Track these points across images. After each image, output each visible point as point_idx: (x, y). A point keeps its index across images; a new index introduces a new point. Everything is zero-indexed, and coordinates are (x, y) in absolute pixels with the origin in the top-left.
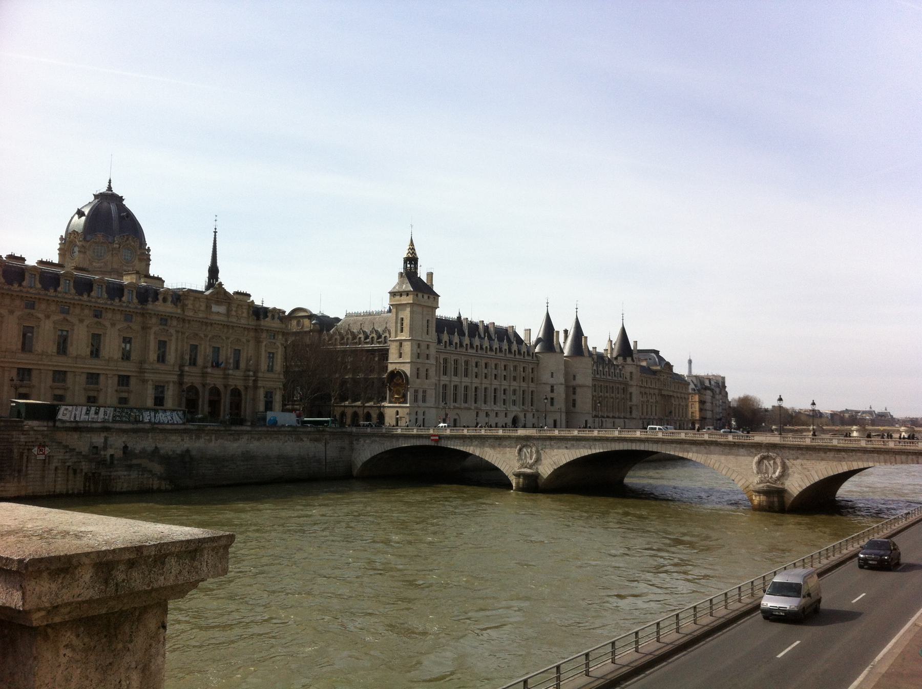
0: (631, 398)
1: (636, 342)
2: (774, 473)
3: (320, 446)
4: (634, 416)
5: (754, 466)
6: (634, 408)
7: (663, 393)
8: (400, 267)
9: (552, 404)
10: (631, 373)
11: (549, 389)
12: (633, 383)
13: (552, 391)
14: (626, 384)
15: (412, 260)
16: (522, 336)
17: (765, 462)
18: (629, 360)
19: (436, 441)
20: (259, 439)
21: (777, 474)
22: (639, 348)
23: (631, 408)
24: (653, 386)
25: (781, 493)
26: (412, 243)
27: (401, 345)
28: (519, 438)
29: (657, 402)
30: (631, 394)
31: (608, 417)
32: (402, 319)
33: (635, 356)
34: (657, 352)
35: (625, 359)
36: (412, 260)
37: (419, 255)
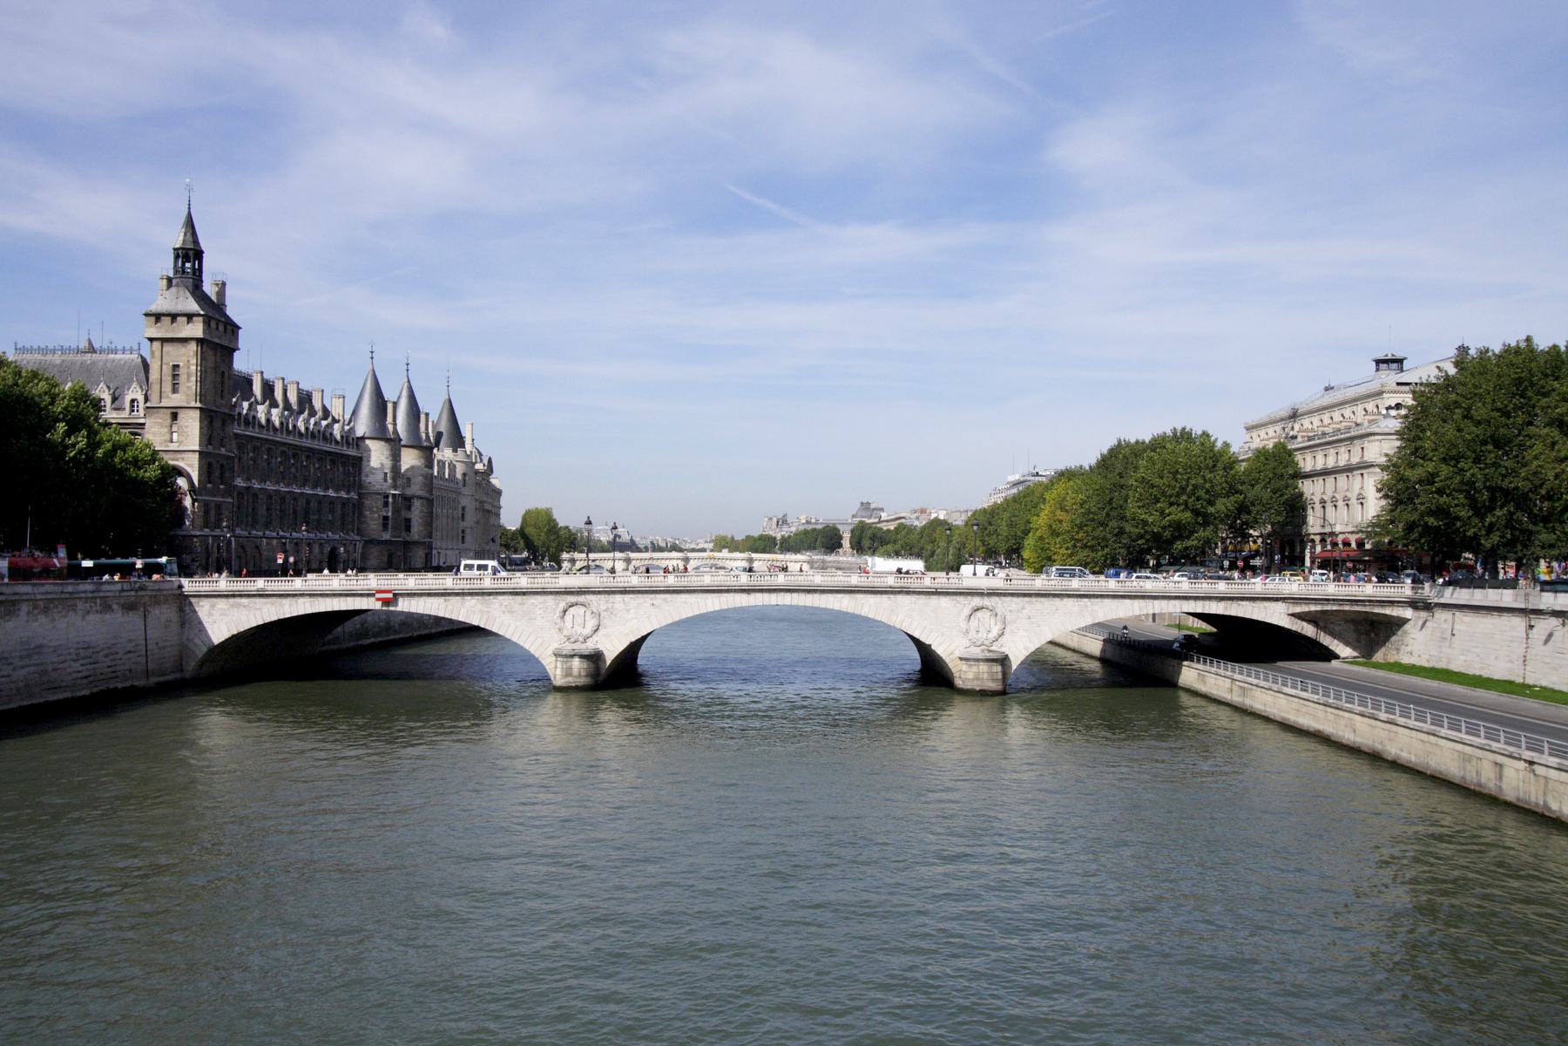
3: (135, 619)
4: (467, 545)
5: (964, 625)
6: (468, 531)
7: (487, 507)
8: (167, 266)
9: (385, 526)
11: (380, 503)
12: (465, 491)
13: (386, 504)
15: (190, 256)
17: (979, 614)
19: (386, 602)
20: (46, 611)
21: (995, 631)
25: (1003, 661)
26: (190, 224)
27: (175, 417)
28: (568, 592)
32: (176, 367)
35: (455, 451)
36: (190, 256)
37: (203, 246)
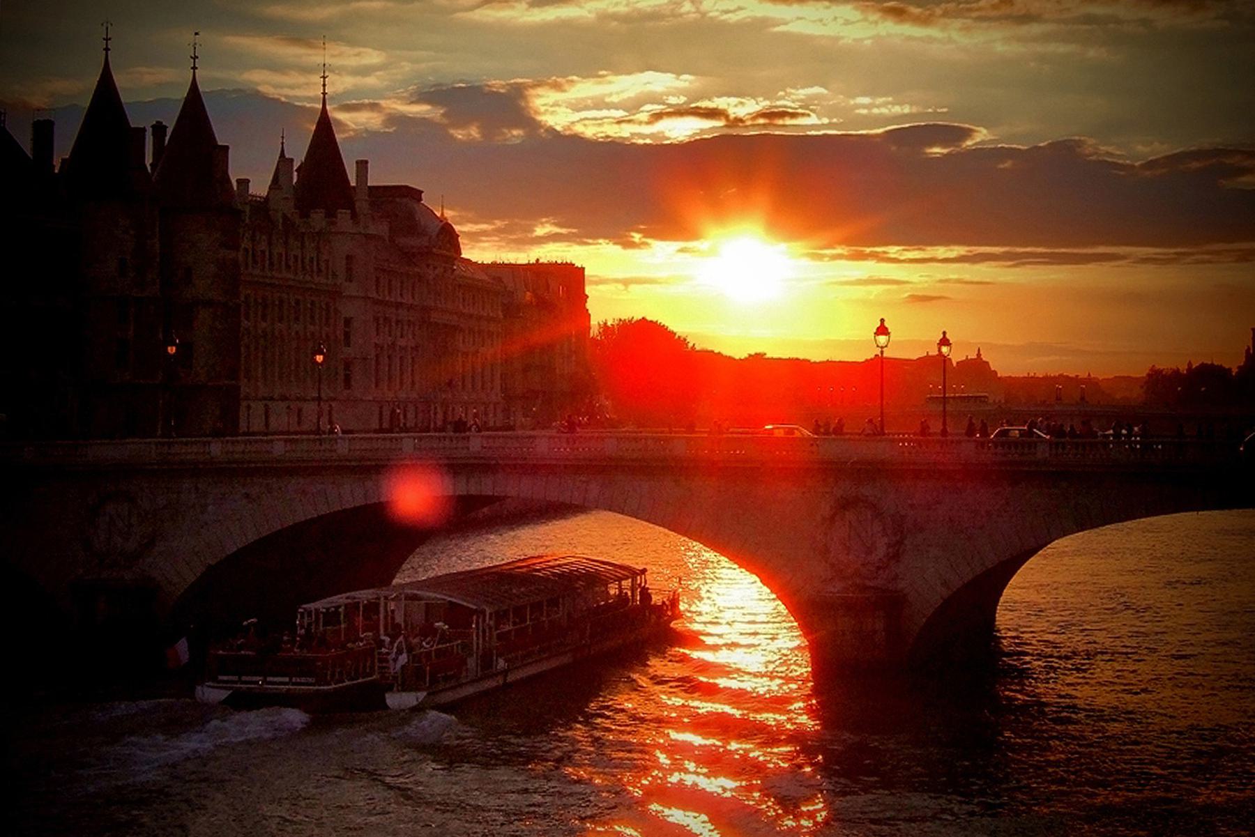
0: (347, 335)
1: (362, 165)
2: (869, 551)
10: (349, 258)
14: (335, 294)
16: (25, 142)
18: (343, 215)
21: (881, 551)
22: (375, 179)
23: (348, 365)
24: (407, 299)
29: (416, 348)
30: (348, 322)
31: (284, 398)
33: (362, 205)
34: (416, 194)
35: (331, 215)
